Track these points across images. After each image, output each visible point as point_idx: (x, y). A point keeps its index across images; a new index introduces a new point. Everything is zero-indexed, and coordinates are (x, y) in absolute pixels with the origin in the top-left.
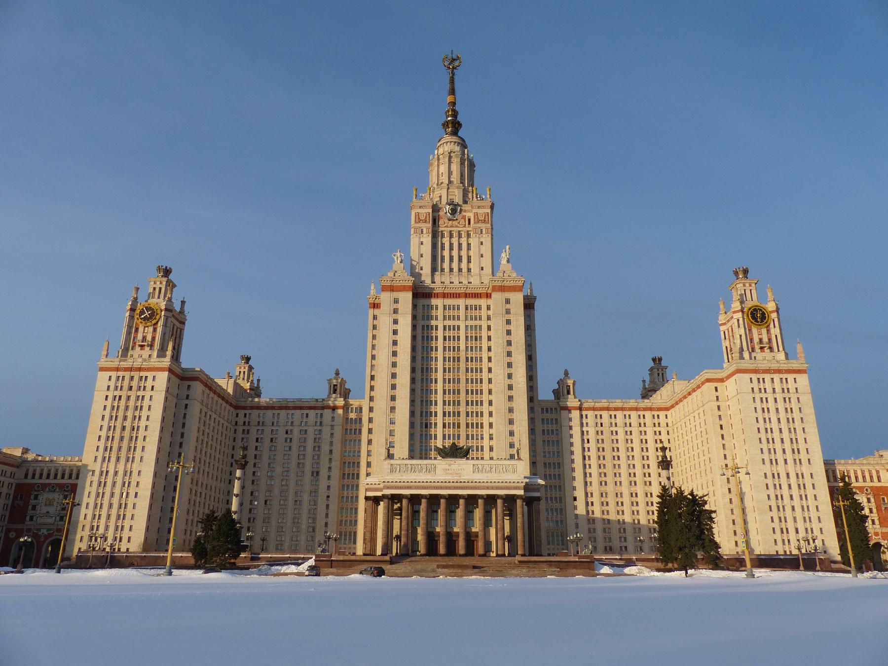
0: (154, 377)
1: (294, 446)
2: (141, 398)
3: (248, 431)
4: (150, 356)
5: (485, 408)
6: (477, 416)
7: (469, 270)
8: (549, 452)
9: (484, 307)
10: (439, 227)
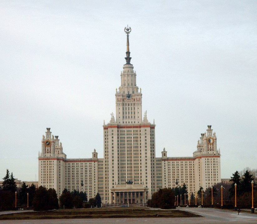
5: (139, 162)
7: (134, 117)
9: (139, 131)
10: (125, 102)
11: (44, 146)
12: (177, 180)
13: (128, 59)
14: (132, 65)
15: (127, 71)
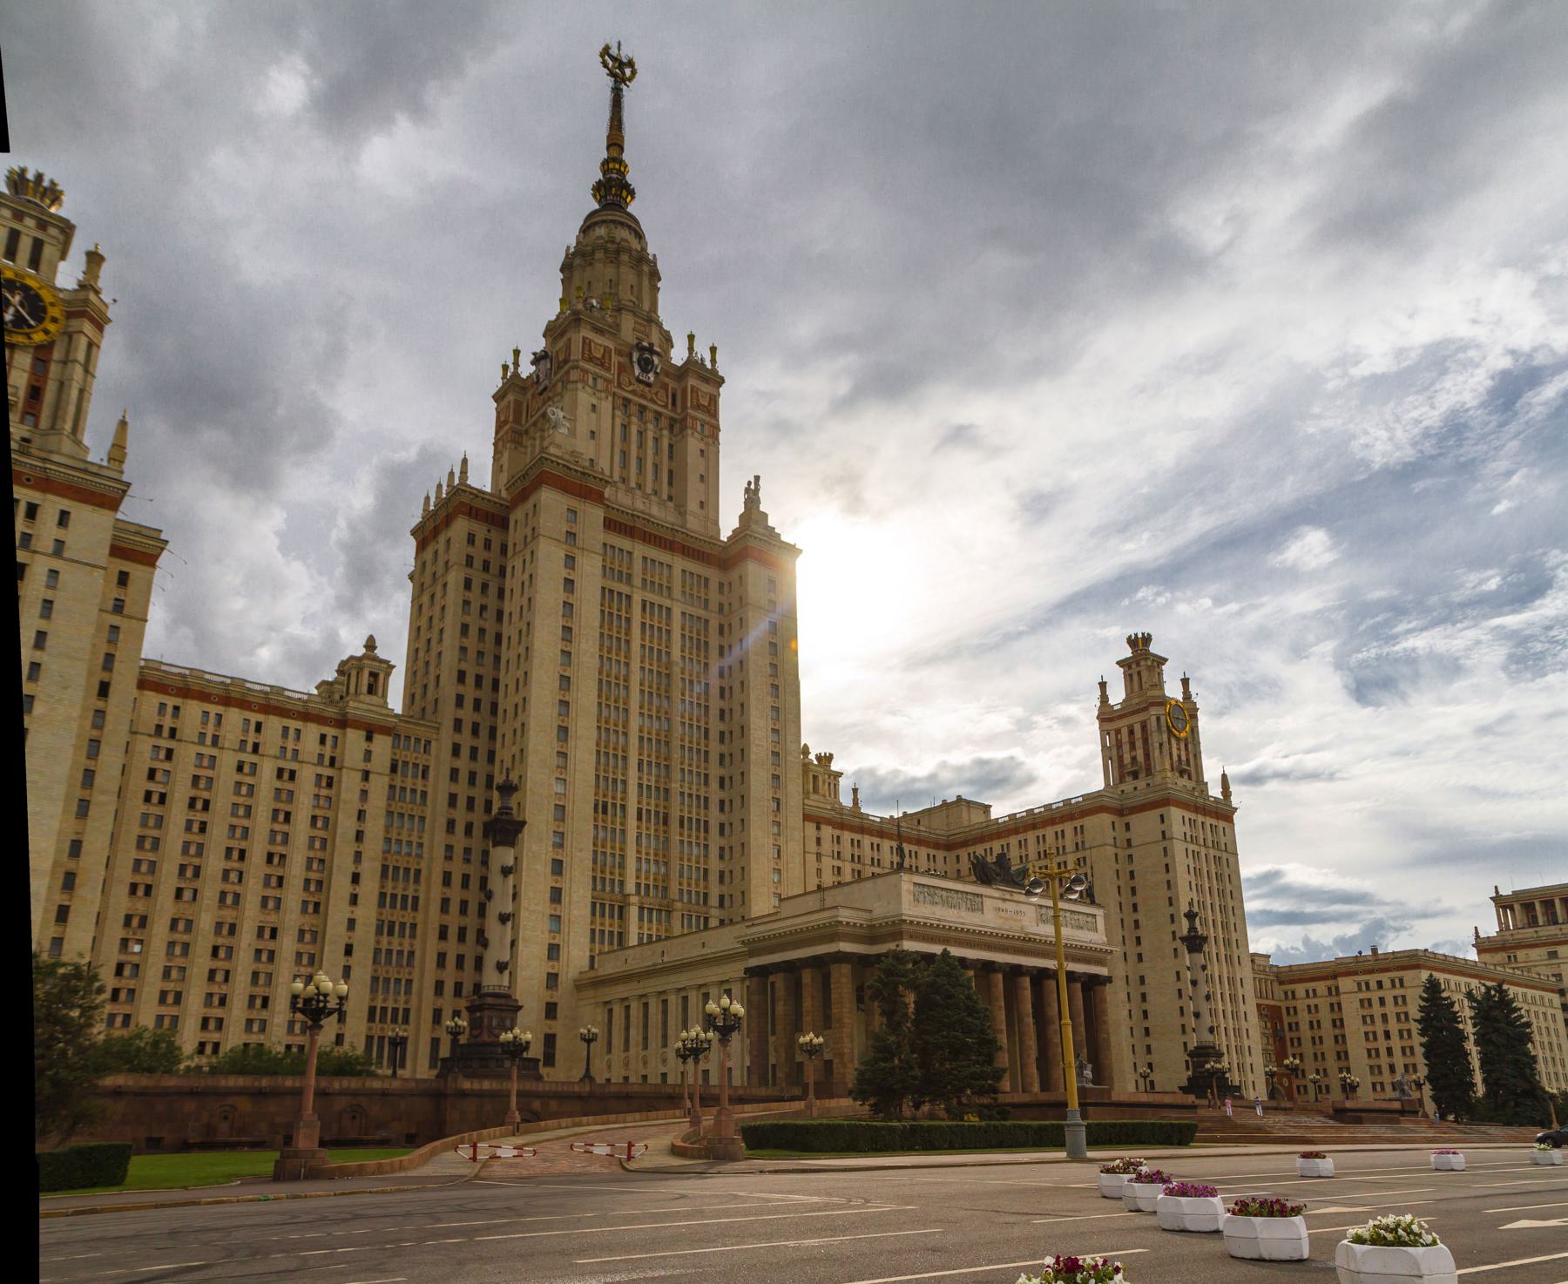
1: (260, 808)
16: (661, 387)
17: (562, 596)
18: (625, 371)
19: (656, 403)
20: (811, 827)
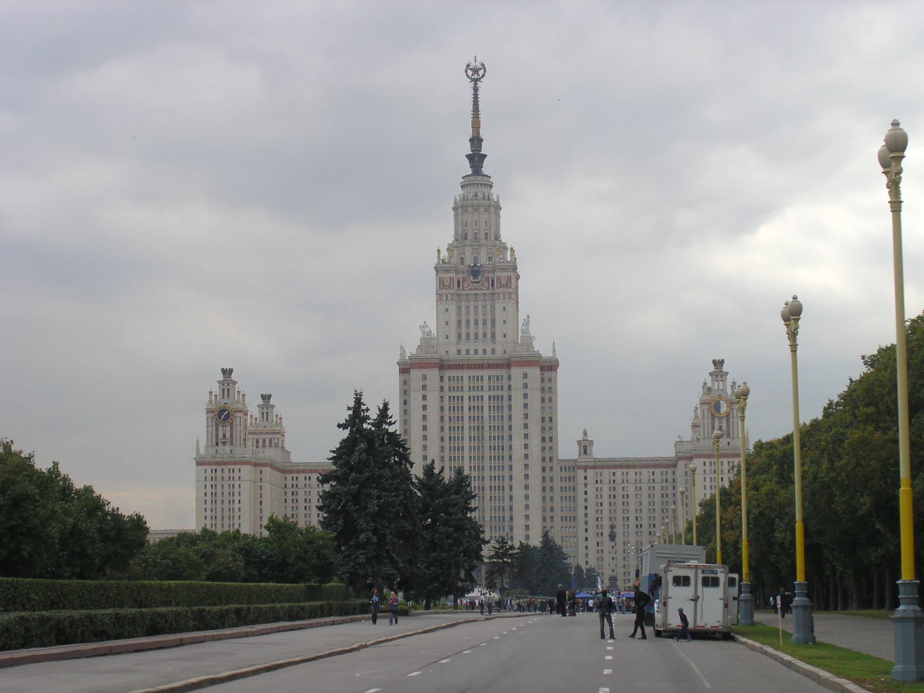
0: (239, 469)
2: (231, 486)
3: (297, 492)
4: (231, 451)
6: (499, 480)
7: (493, 336)
8: (566, 507)
11: (214, 424)
12: (612, 527)
13: (476, 159)
14: (490, 177)
15: (470, 196)
16: (485, 280)
17: (422, 413)
18: (466, 281)
19: (483, 290)
20: (583, 470)
